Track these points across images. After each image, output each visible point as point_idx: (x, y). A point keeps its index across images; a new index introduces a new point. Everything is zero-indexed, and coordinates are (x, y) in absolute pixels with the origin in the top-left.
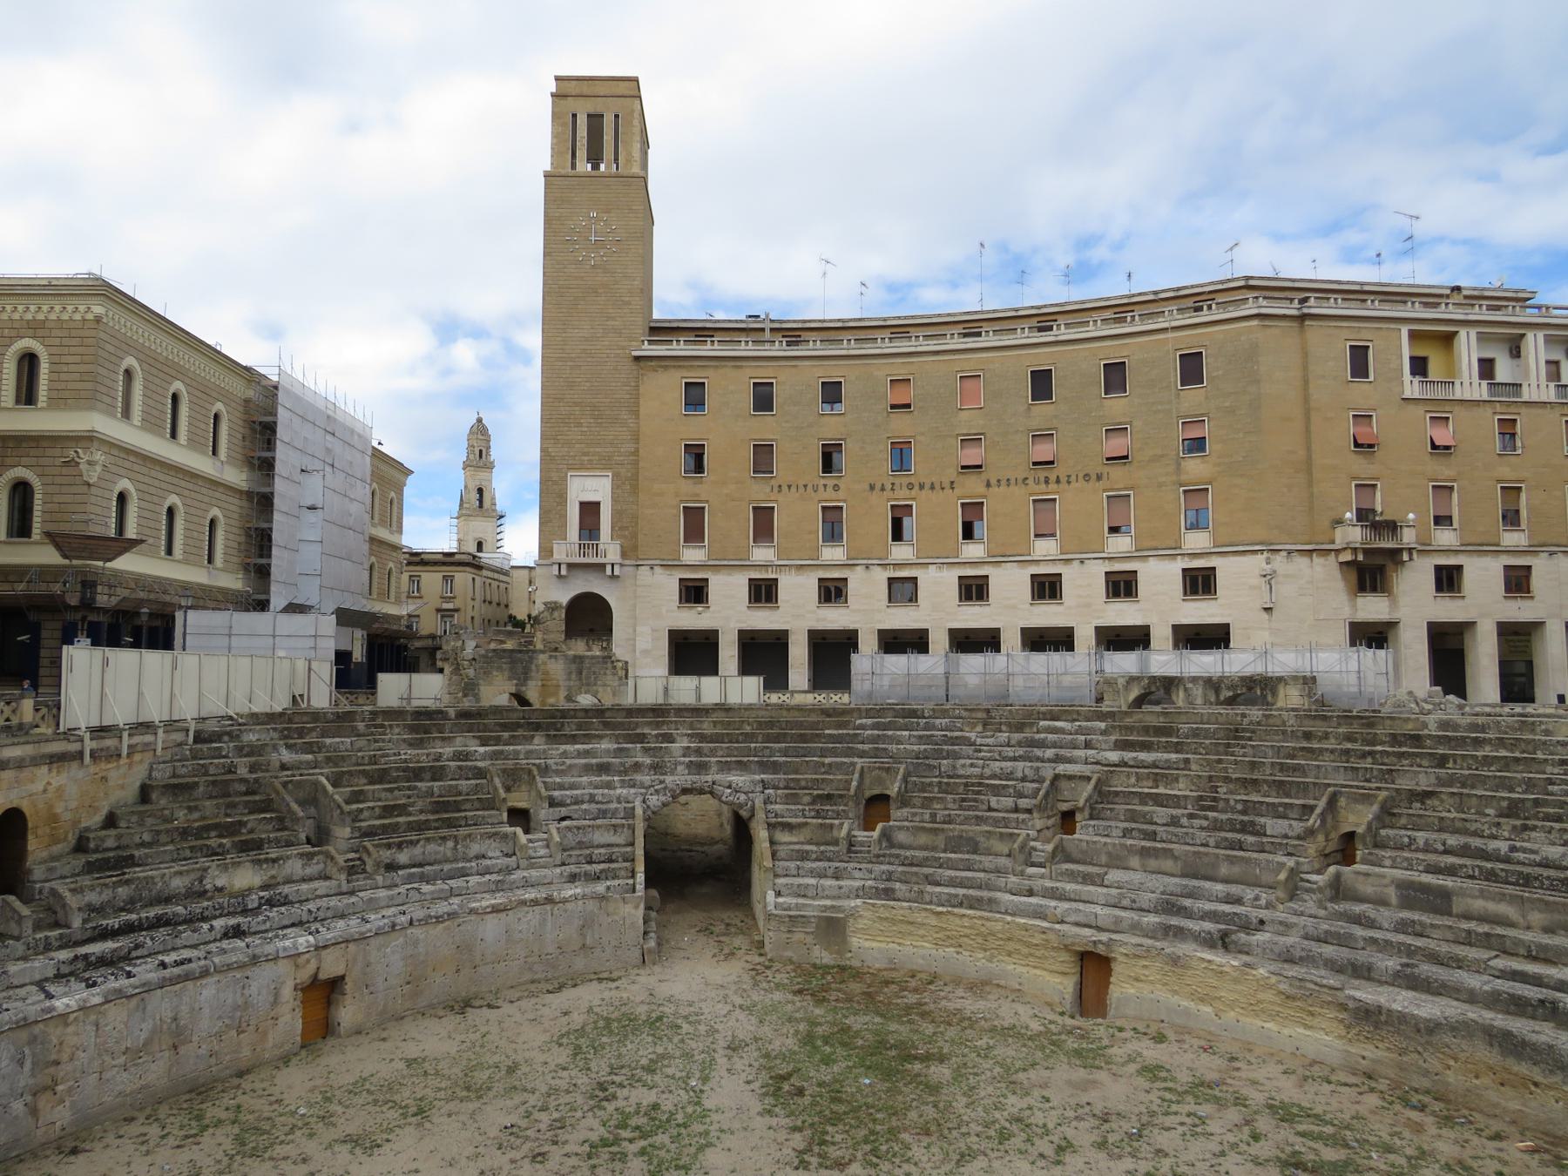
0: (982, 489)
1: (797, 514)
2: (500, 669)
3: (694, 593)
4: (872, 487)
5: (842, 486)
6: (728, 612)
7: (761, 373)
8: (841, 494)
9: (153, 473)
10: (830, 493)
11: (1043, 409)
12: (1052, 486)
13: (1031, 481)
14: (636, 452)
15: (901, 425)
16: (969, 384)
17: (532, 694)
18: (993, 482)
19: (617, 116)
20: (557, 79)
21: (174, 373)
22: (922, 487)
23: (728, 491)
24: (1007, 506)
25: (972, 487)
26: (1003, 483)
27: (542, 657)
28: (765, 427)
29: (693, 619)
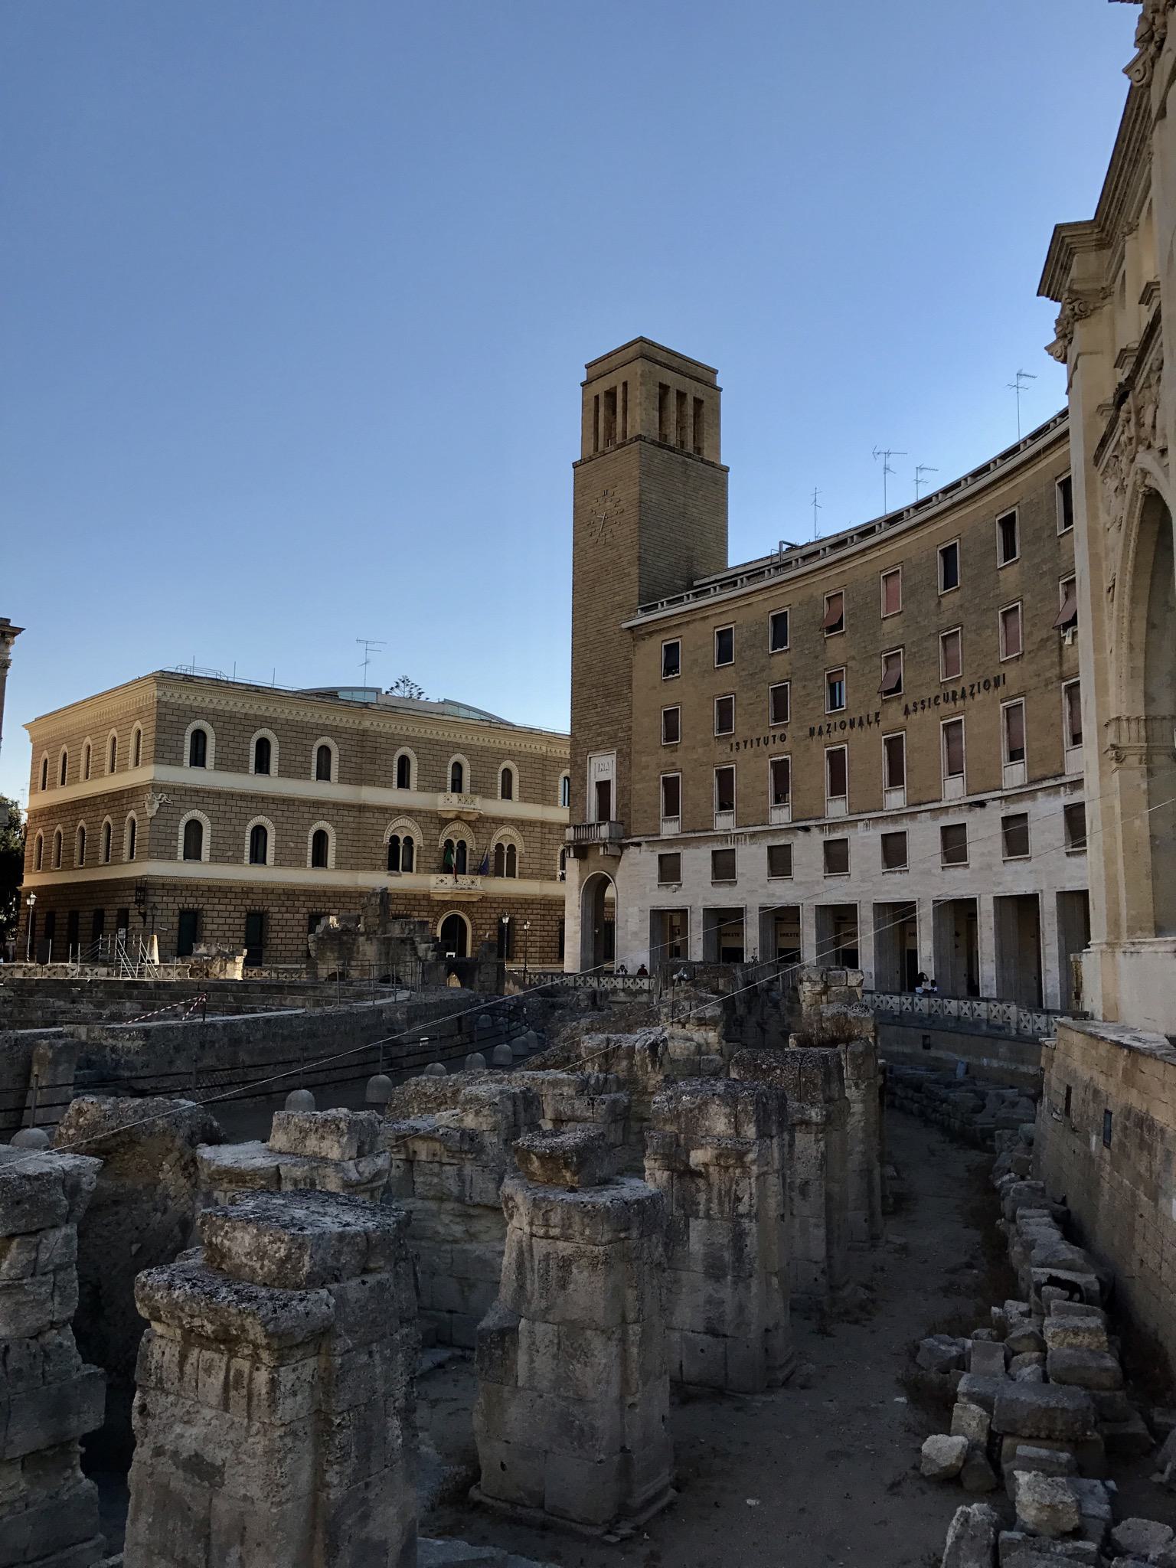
0: (902, 719)
1: (753, 774)
2: (332, 951)
3: (670, 871)
4: (812, 732)
5: (788, 735)
6: (697, 891)
7: (724, 619)
8: (787, 745)
9: (233, 803)
10: (777, 746)
11: (952, 599)
12: (960, 703)
13: (940, 701)
14: (630, 728)
15: (837, 649)
16: (892, 581)
17: (354, 974)
18: (911, 707)
19: (625, 384)
20: (588, 367)
21: (258, 724)
22: (852, 725)
23: (698, 756)
24: (923, 734)
25: (894, 713)
26: (919, 706)
27: (362, 939)
28: (727, 680)
29: (668, 899)
